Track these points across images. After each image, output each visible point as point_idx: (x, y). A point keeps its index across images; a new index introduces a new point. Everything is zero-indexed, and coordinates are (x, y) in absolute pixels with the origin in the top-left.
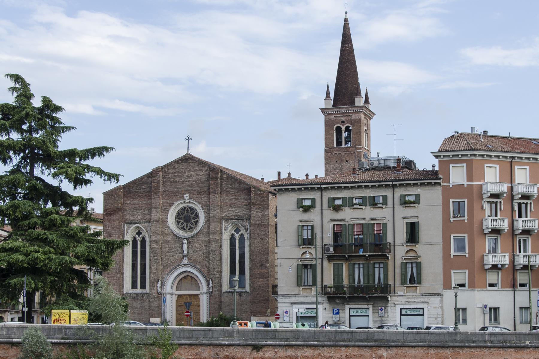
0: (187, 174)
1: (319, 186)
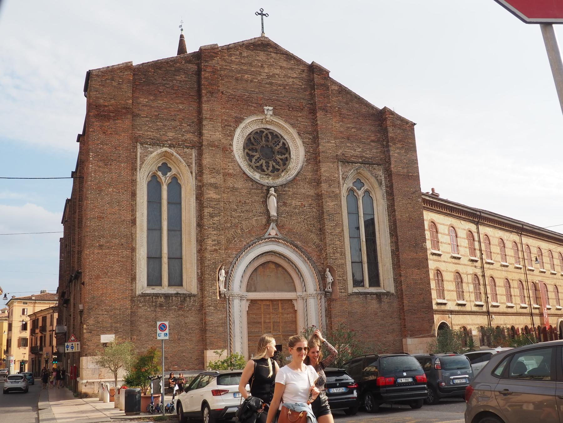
0: (266, 70)
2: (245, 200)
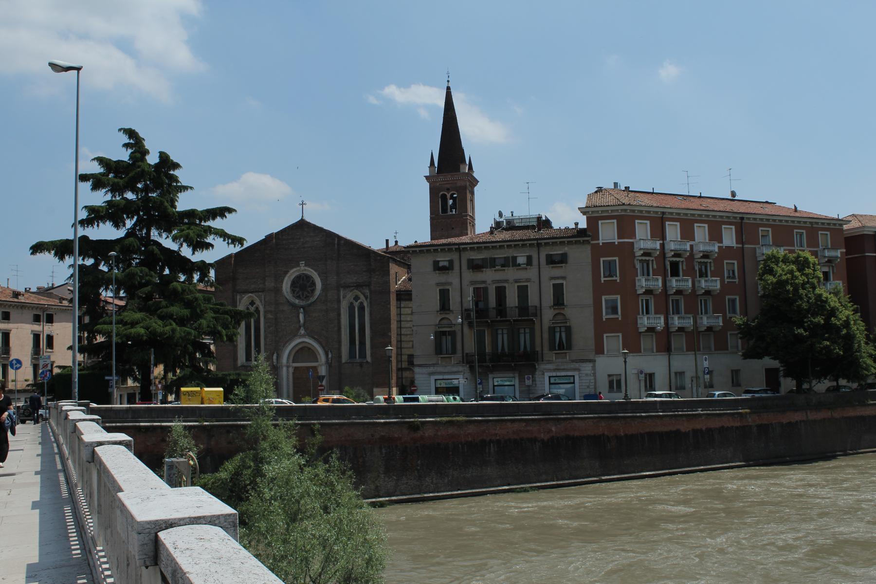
1: (457, 247)
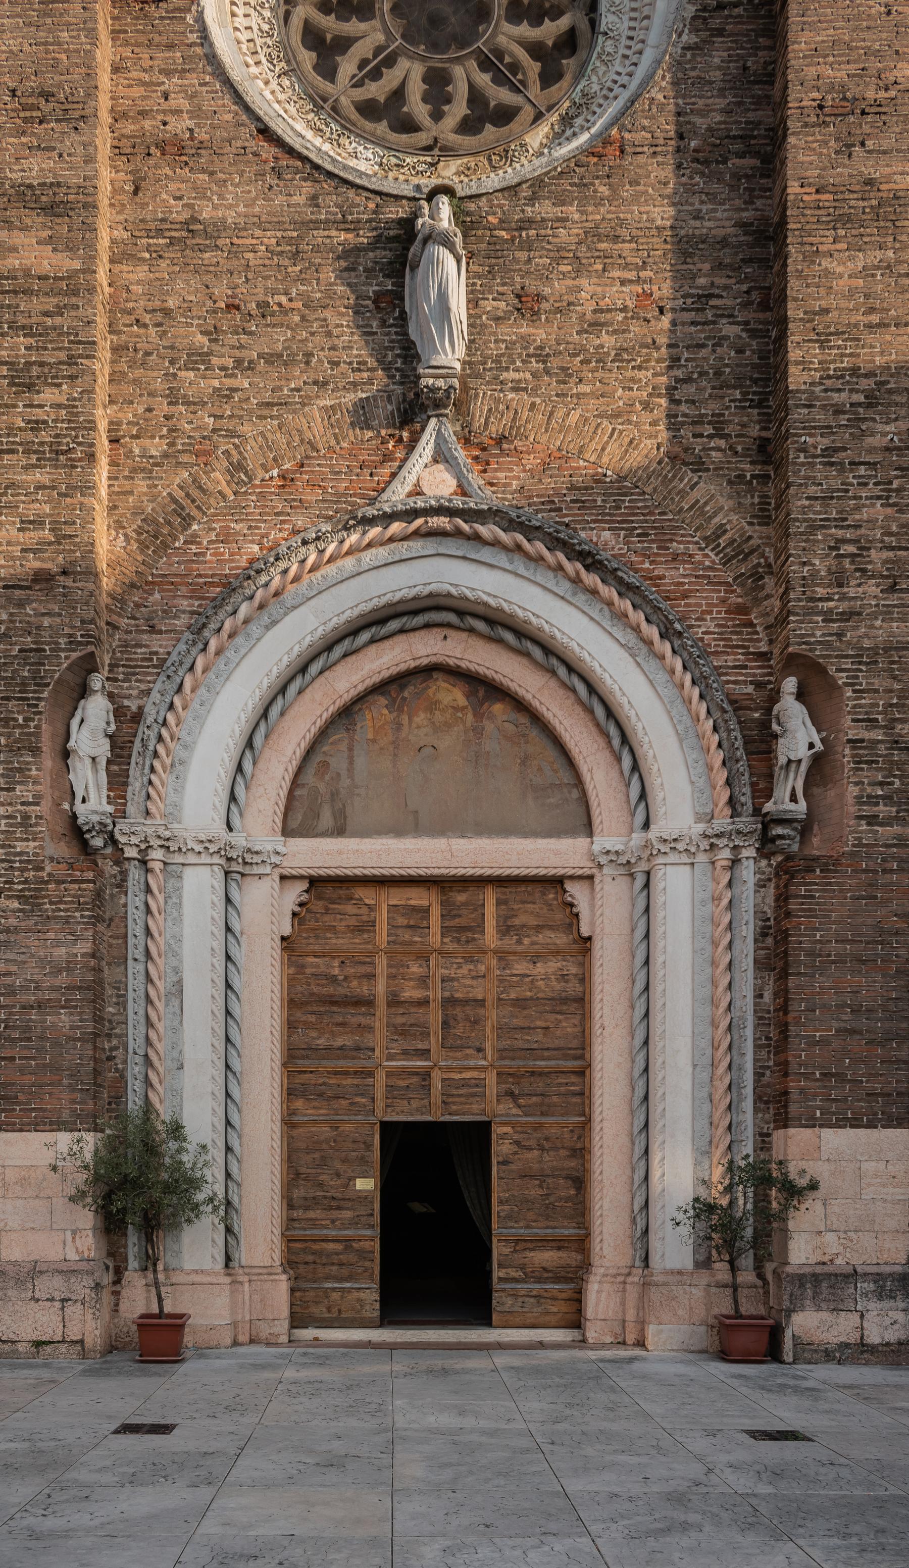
2: (261, 298)
